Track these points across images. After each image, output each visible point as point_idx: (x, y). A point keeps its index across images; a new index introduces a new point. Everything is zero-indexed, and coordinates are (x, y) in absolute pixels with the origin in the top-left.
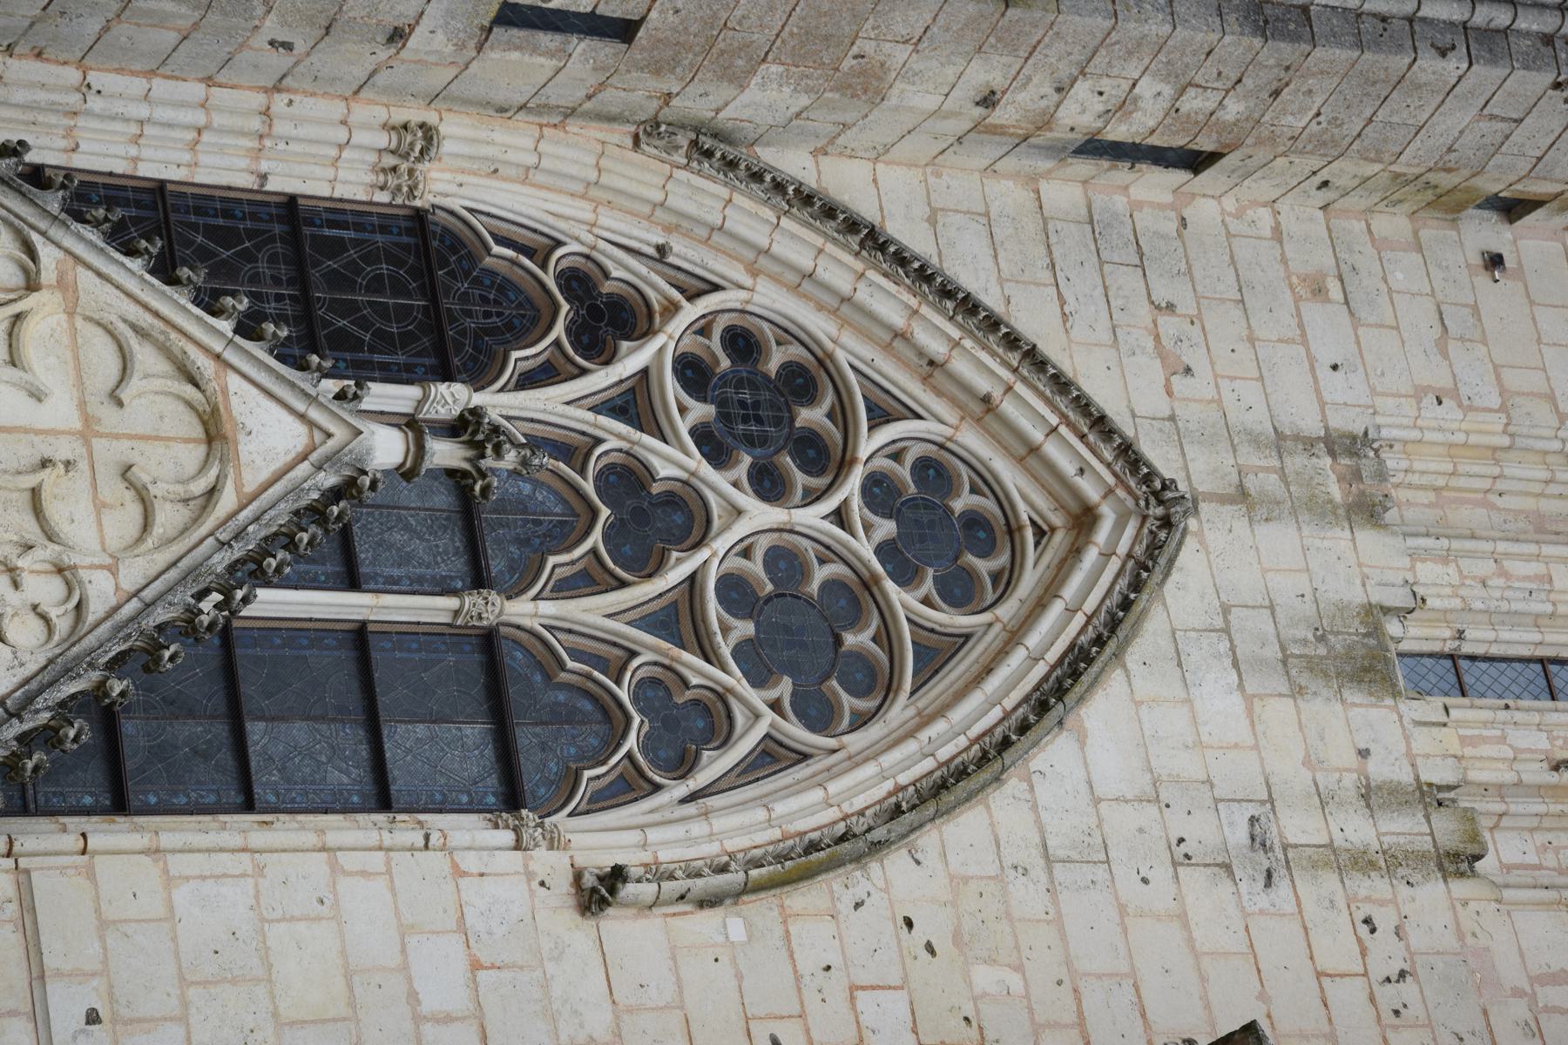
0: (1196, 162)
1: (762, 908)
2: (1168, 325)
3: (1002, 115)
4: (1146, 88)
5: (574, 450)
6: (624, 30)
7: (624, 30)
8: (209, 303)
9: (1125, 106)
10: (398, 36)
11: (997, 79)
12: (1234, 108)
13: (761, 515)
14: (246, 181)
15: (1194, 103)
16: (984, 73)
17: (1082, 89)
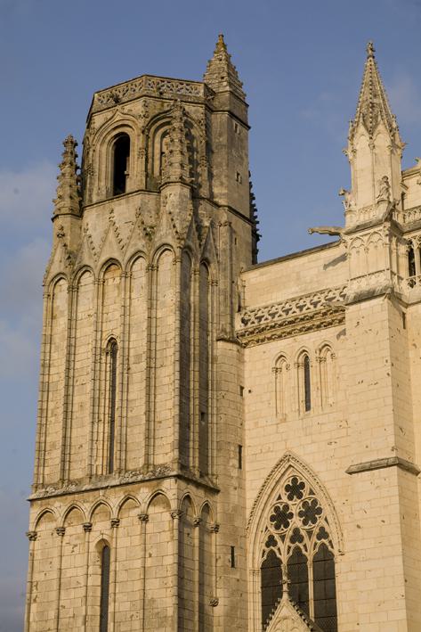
0: (240, 447)
1: (343, 526)
2: (264, 451)
3: (237, 485)
4: (231, 464)
5: (289, 547)
6: (233, 548)
7: (233, 548)
8: (271, 619)
9: (233, 466)
10: (238, 580)
11: (232, 488)
12: (232, 448)
13: (294, 519)
14: (260, 594)
15: (232, 455)
16: (232, 492)
17: (232, 475)
